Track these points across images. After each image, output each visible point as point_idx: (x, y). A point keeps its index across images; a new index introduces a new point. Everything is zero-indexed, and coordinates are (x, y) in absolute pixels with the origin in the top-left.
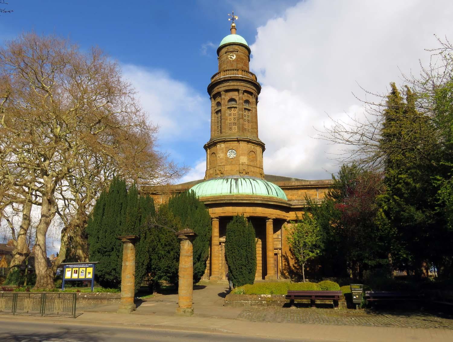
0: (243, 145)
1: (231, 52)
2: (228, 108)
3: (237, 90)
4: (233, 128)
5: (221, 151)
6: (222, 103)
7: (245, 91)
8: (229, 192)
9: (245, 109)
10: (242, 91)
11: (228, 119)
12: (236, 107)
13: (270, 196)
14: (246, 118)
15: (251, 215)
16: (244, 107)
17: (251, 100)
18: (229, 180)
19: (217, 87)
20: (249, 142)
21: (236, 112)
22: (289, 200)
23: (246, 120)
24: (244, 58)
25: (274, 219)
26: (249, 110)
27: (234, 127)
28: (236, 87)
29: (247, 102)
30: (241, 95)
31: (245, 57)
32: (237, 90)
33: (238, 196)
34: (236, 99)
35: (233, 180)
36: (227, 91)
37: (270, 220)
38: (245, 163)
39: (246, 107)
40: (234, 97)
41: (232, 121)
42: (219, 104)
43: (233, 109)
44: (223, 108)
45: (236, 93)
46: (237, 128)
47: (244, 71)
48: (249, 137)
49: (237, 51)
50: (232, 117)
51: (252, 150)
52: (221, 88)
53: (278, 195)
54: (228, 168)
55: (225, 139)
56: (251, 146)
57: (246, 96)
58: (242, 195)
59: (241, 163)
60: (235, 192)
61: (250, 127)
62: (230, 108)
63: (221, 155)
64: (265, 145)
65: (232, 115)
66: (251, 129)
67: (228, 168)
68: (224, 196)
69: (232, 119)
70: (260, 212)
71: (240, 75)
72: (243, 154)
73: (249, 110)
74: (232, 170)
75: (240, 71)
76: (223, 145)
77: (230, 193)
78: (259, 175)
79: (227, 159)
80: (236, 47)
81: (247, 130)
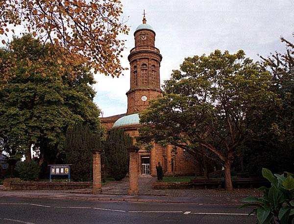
6: (138, 66)
17: (156, 65)
28: (146, 57)
42: (135, 67)
44: (139, 70)
52: (137, 57)
57: (153, 63)
75: (149, 47)
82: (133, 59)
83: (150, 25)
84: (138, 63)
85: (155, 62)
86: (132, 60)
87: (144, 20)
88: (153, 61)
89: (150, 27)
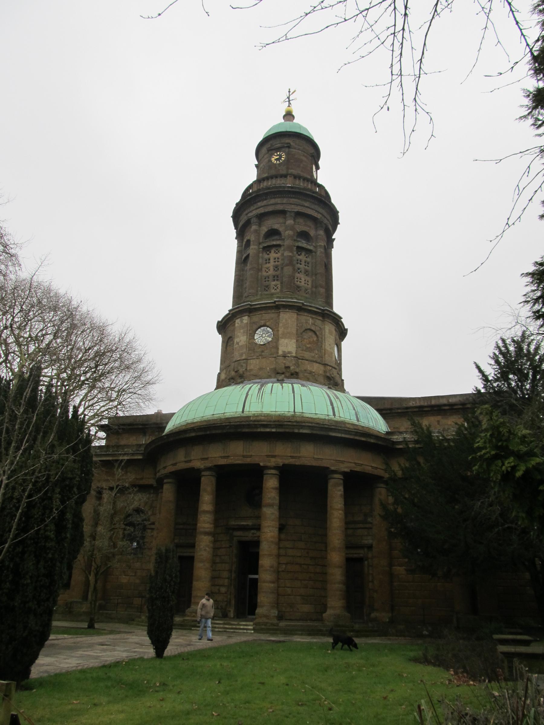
1: (278, 149)
2: (264, 248)
3: (283, 213)
4: (272, 286)
5: (242, 331)
7: (299, 214)
9: (300, 249)
10: (293, 214)
11: (264, 269)
12: (279, 246)
13: (337, 418)
14: (302, 267)
15: (287, 462)
16: (297, 244)
17: (312, 233)
20: (300, 309)
22: (388, 433)
23: (303, 271)
24: (304, 158)
25: (344, 474)
26: (308, 251)
27: (274, 283)
28: (280, 207)
29: (304, 235)
30: (290, 222)
31: (306, 157)
32: (283, 213)
33: (258, 418)
34: (281, 229)
36: (261, 217)
38: (290, 353)
39: (300, 244)
40: (276, 227)
41: (271, 272)
45: (281, 220)
46: (279, 286)
47: (299, 179)
49: (289, 147)
51: (309, 327)
53: (358, 420)
54: (254, 364)
55: (251, 305)
56: (309, 321)
57: (302, 226)
58: (268, 415)
59: (280, 352)
61: (310, 283)
62: (267, 249)
63: (241, 339)
64: (341, 318)
65: (272, 261)
66: (312, 287)
67: (254, 364)
69: (272, 269)
70: (308, 455)
71: (289, 183)
72: (285, 336)
73: (308, 251)
74: (261, 369)
76: (246, 319)
77: (243, 412)
78: (321, 379)
79: (252, 346)
83: (306, 122)
84: (254, 227)
85: (310, 223)
87: (289, 116)
88: (301, 220)
89: (300, 127)
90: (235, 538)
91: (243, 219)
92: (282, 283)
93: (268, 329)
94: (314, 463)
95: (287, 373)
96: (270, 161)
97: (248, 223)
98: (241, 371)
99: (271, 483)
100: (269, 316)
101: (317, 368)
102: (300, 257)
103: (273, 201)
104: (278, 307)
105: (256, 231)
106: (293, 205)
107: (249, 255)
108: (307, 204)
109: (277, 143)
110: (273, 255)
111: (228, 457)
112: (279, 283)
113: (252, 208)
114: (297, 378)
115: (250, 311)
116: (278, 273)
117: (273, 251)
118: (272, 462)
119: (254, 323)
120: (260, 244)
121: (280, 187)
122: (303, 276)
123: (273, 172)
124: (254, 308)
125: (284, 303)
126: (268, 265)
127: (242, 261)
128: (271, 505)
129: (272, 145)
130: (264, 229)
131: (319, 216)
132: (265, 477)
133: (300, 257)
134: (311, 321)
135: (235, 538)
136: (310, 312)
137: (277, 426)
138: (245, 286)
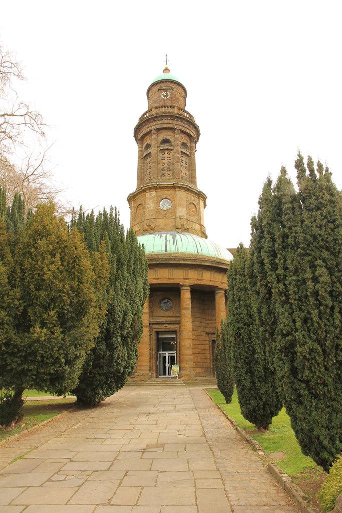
0: (181, 195)
1: (165, 90)
2: (161, 150)
3: (173, 129)
6: (153, 143)
7: (182, 132)
8: (164, 249)
10: (179, 131)
12: (171, 150)
17: (189, 144)
18: (164, 236)
19: (147, 126)
21: (170, 155)
28: (172, 126)
29: (184, 145)
30: (178, 136)
32: (173, 129)
33: (176, 255)
35: (168, 235)
36: (159, 130)
37: (221, 291)
40: (168, 138)
43: (166, 152)
44: (153, 150)
48: (188, 184)
49: (172, 89)
50: (166, 161)
52: (153, 126)
54: (161, 222)
57: (185, 140)
58: (182, 254)
59: (177, 216)
60: (172, 249)
62: (163, 151)
63: (150, 205)
65: (166, 158)
66: (189, 177)
67: (161, 222)
68: (156, 255)
69: (166, 163)
70: (208, 278)
71: (176, 111)
74: (165, 225)
76: (153, 193)
77: (166, 251)
78: (199, 233)
79: (159, 211)
80: (171, 85)
81: (185, 178)
82: (145, 130)
84: (154, 136)
85: (187, 138)
86: (142, 134)
88: (183, 136)
90: (154, 329)
91: (145, 130)
92: (173, 173)
93: (168, 200)
94: (211, 284)
95: (184, 229)
96: (160, 96)
97: (149, 133)
98: (153, 226)
99: (186, 295)
100: (169, 192)
101: (197, 227)
102: (183, 158)
103: (166, 121)
104: (174, 187)
105: (155, 139)
106: (179, 125)
107: (150, 153)
108: (187, 126)
109: (164, 86)
110: (166, 155)
111: (158, 279)
112: (171, 173)
113: (152, 124)
114: (188, 232)
115: (157, 188)
116: (170, 166)
117: (166, 152)
118: (188, 283)
119: (159, 196)
120: (158, 147)
121: (172, 113)
122: (183, 170)
123: (162, 104)
124: (159, 187)
125: (179, 185)
126: (163, 161)
127: (144, 157)
128: (187, 309)
129: (161, 87)
130: (161, 138)
131: (193, 135)
132: (182, 292)
133: (183, 158)
134: (193, 198)
135: (154, 329)
136: (193, 192)
137: (194, 260)
138: (146, 173)
